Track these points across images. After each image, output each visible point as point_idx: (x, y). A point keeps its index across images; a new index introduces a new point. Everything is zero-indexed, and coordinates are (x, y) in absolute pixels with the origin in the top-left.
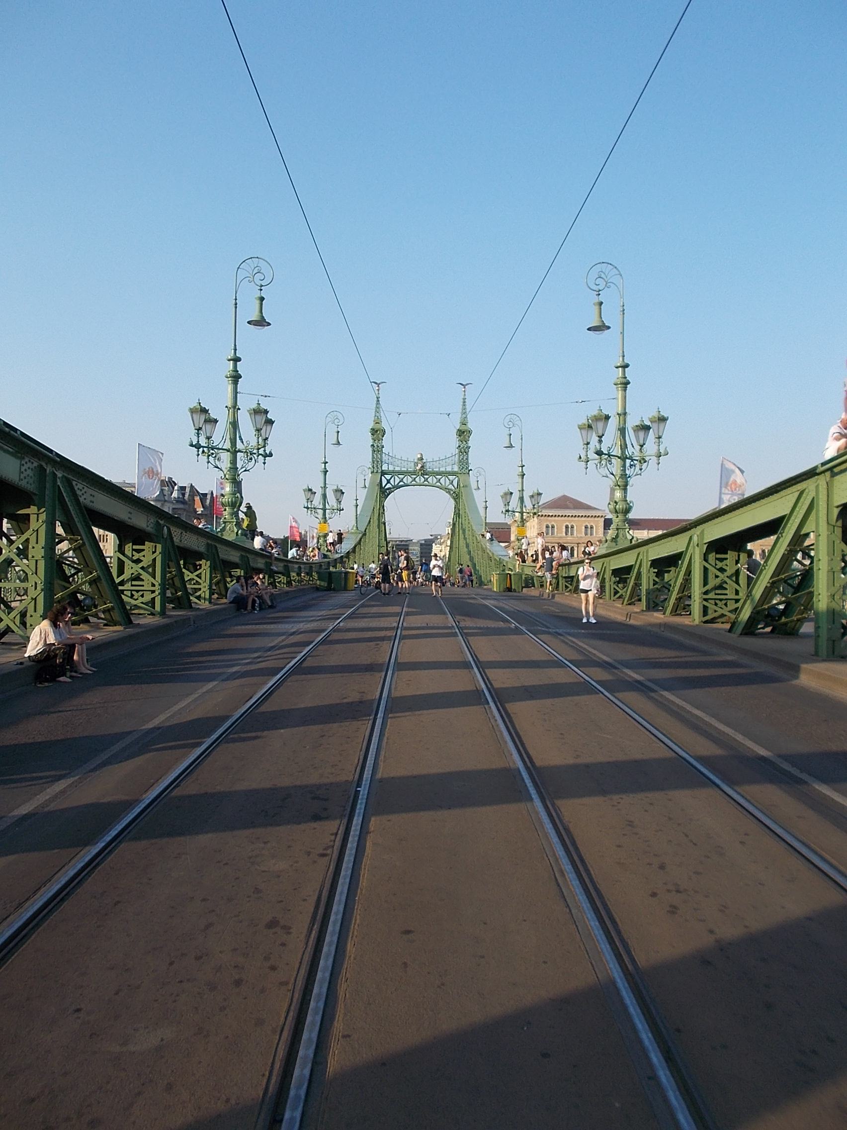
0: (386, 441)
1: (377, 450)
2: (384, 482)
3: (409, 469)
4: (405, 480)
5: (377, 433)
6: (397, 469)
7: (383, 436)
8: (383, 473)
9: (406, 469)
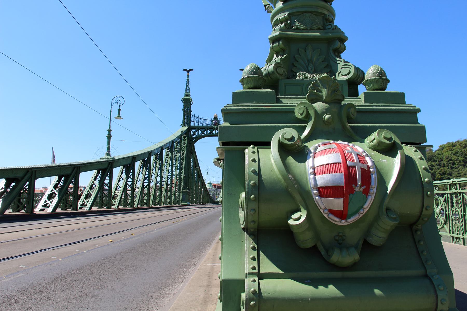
0: (193, 108)
1: (187, 113)
2: (192, 133)
3: (208, 125)
4: (205, 133)
5: (187, 102)
6: (200, 125)
7: (192, 104)
8: (190, 128)
9: (206, 125)
